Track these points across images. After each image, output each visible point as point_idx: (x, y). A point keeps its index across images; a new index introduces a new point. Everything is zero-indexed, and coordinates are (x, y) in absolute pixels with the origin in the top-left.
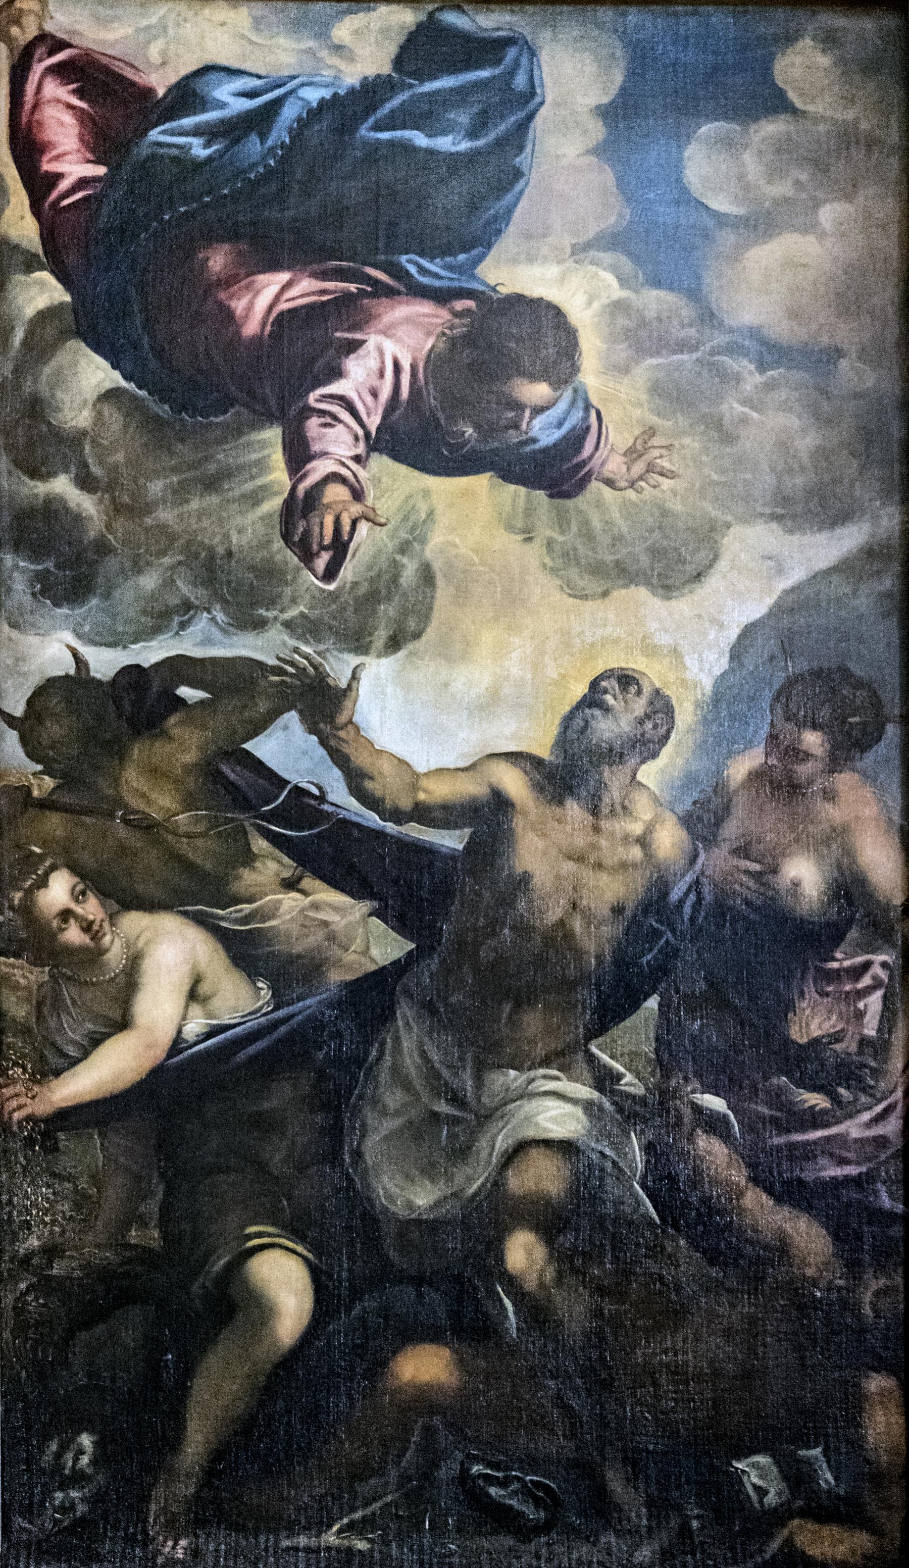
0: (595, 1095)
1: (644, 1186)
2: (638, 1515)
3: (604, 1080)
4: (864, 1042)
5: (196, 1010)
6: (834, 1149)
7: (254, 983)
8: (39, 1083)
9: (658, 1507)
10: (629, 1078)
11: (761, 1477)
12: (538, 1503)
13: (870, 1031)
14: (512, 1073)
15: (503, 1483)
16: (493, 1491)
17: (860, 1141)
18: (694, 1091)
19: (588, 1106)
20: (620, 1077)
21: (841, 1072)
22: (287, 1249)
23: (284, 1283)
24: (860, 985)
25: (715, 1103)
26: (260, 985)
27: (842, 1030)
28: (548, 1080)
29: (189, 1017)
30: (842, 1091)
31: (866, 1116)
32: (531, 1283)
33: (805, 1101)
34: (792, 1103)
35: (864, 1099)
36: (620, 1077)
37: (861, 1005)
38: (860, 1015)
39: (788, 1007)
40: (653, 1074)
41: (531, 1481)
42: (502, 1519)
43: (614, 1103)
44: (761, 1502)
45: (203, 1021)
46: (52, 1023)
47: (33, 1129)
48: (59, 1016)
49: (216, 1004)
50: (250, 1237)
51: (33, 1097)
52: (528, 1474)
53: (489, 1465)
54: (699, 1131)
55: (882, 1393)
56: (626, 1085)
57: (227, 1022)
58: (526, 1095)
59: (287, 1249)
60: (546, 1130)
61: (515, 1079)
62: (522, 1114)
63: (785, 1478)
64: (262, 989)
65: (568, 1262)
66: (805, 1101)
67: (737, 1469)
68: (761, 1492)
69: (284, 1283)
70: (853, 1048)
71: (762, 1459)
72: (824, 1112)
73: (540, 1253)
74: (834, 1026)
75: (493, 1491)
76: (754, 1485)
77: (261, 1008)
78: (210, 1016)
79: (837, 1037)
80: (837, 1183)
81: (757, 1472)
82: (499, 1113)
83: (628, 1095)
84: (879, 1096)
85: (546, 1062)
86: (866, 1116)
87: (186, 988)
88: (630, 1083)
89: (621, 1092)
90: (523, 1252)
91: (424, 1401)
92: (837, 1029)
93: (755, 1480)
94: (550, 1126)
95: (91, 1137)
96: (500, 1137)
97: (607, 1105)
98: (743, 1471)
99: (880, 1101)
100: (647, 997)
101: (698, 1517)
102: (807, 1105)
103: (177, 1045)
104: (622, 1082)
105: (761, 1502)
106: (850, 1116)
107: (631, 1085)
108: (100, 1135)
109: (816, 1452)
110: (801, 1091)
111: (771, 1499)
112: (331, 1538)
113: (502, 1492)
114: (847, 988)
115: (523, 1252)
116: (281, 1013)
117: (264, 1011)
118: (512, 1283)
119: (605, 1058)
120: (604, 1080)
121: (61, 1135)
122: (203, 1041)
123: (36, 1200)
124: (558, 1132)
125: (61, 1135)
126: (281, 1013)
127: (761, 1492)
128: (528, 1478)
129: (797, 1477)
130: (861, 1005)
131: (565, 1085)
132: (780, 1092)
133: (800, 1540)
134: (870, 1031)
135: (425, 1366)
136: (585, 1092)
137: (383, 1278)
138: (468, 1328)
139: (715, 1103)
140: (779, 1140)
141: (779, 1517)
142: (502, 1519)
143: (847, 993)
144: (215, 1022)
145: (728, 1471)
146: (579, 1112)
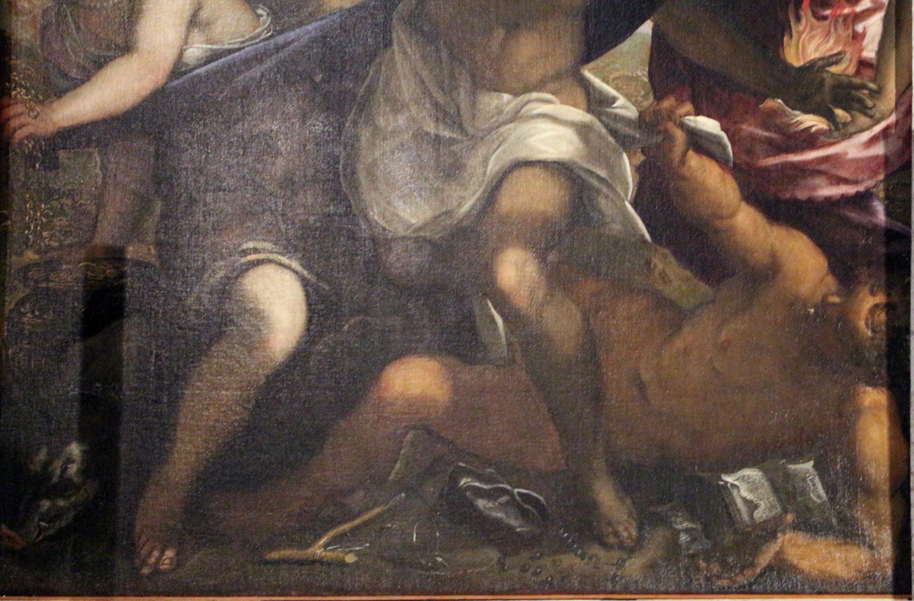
0: (587, 118)
1: (635, 204)
2: (628, 530)
3: (597, 103)
4: (863, 64)
5: (196, 35)
6: (827, 169)
7: (254, 10)
8: (42, 103)
9: (647, 519)
10: (621, 101)
11: (751, 491)
12: (524, 514)
13: (870, 52)
14: (506, 97)
15: (488, 495)
16: (481, 503)
17: (856, 161)
18: (688, 114)
19: (583, 131)
20: (614, 99)
21: (842, 96)
22: (281, 265)
23: (278, 301)
24: (859, 9)
25: (709, 125)
26: (260, 11)
27: (839, 53)
28: (545, 103)
29: (190, 40)
30: (839, 112)
31: (865, 136)
32: (521, 300)
33: (801, 123)
34: (789, 125)
35: (863, 120)
36: (614, 99)
37: (859, 28)
38: (857, 37)
39: (784, 28)
40: (645, 97)
41: (519, 493)
42: (488, 531)
43: (607, 126)
44: (751, 516)
45: (204, 46)
46: (56, 46)
47: (34, 147)
48: (63, 39)
49: (217, 29)
50: (245, 253)
51: (36, 117)
52: (516, 487)
53: (480, 478)
54: (691, 153)
55: (876, 406)
56: (621, 107)
57: (227, 47)
58: (516, 117)
59: (281, 265)
60: (541, 152)
61: (508, 103)
62: (513, 137)
63: (775, 490)
64: (262, 16)
65: (557, 278)
66: (801, 123)
67: (727, 483)
68: (752, 506)
69: (278, 301)
70: (851, 70)
71: (753, 473)
72: (820, 132)
73: (532, 269)
74: (831, 49)
75: (481, 503)
76: (745, 500)
77: (259, 35)
78: (208, 41)
79: (835, 59)
80: (829, 201)
81: (747, 486)
82: (494, 135)
83: (623, 119)
84: (878, 115)
85: (540, 86)
86: (865, 136)
87: (187, 14)
88: (625, 108)
89: (616, 115)
90: (515, 270)
91: (425, 427)
92: (835, 51)
93: (745, 493)
94: (542, 147)
95: (90, 155)
96: (493, 158)
97: (598, 125)
98: (732, 485)
99: (878, 122)
100: (642, 22)
101: (687, 531)
102: (802, 127)
103: (178, 69)
104: (615, 105)
105: (751, 516)
106: (848, 136)
107: (621, 107)
108: (99, 152)
109: (807, 467)
110: (797, 112)
111: (760, 514)
112: (318, 550)
113: (490, 505)
114: (846, 11)
115: (515, 270)
116: (280, 39)
117: (263, 37)
118: (502, 301)
119: (597, 82)
120: (597, 103)
121: (62, 154)
122: (206, 64)
123: (35, 215)
124: (551, 152)
125: (62, 154)
126: (280, 39)
127: (752, 506)
128: (516, 490)
129: (786, 491)
130: (859, 28)
131: (558, 108)
132: (773, 113)
133: (793, 555)
134: (870, 52)
135: (415, 379)
136: (579, 115)
137: (376, 298)
138: (460, 342)
139: (709, 125)
140: (772, 161)
141: (769, 531)
142: (488, 531)
143: (846, 17)
144: (215, 47)
145: (718, 485)
146: (570, 134)
